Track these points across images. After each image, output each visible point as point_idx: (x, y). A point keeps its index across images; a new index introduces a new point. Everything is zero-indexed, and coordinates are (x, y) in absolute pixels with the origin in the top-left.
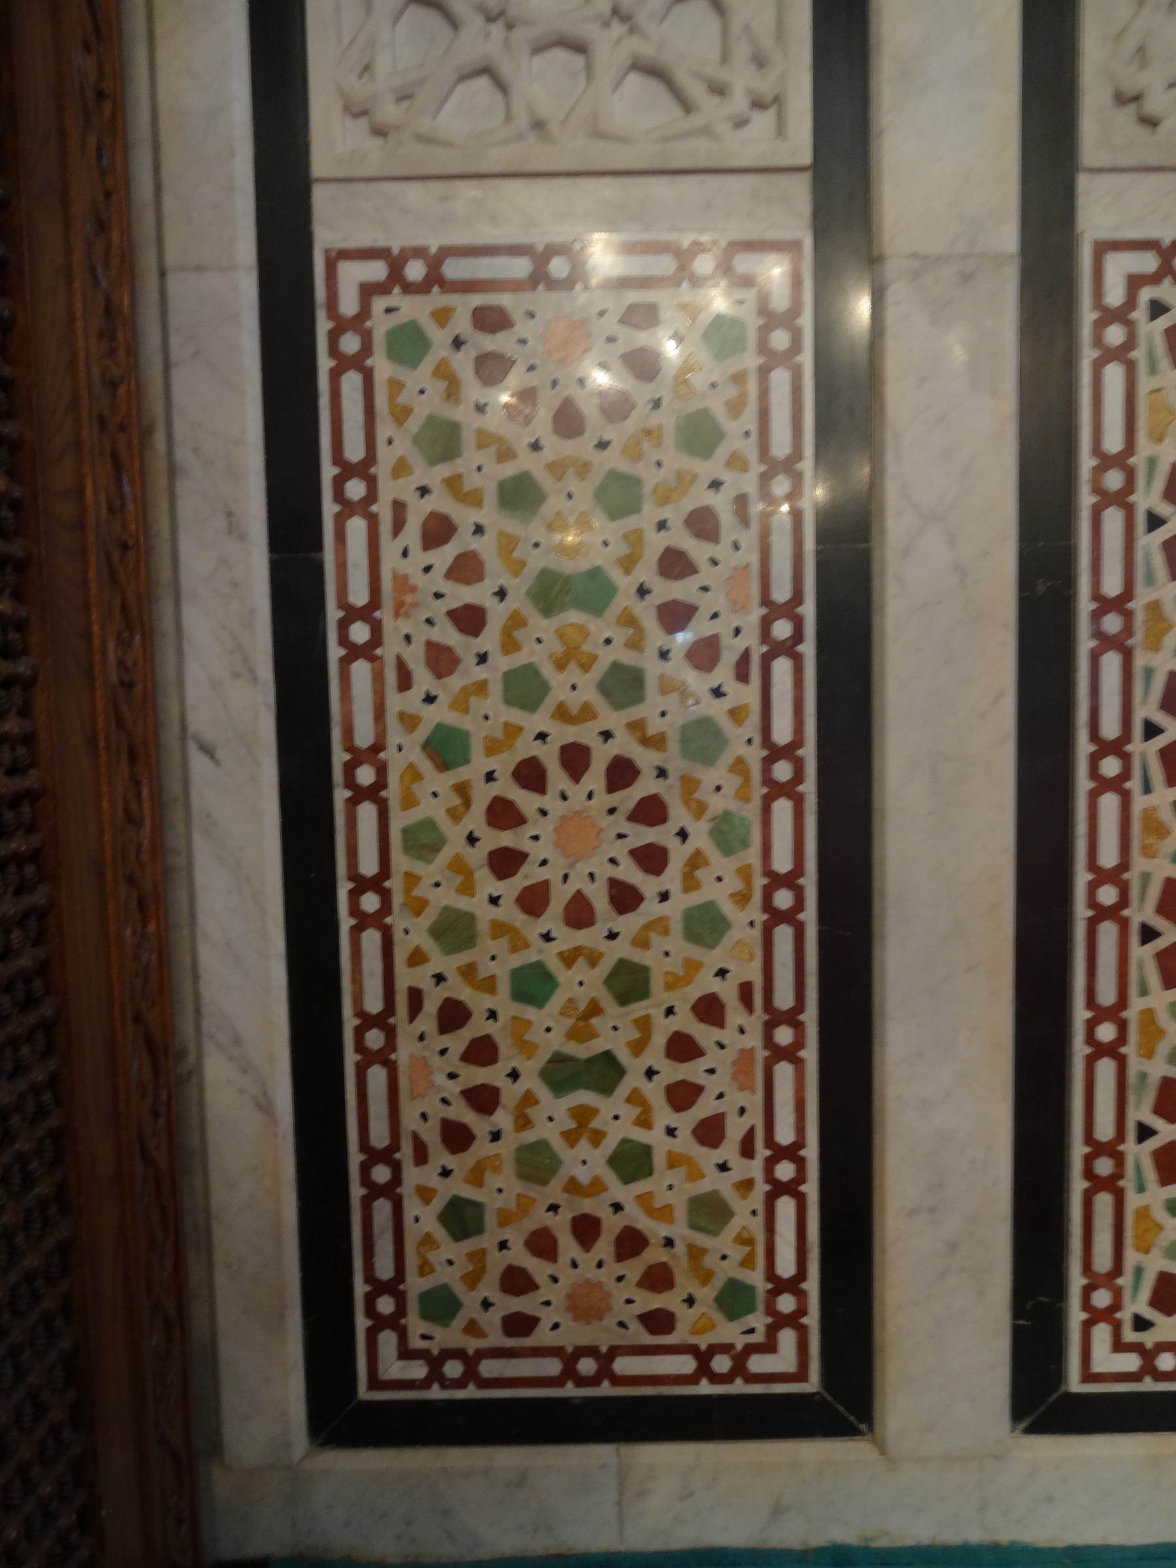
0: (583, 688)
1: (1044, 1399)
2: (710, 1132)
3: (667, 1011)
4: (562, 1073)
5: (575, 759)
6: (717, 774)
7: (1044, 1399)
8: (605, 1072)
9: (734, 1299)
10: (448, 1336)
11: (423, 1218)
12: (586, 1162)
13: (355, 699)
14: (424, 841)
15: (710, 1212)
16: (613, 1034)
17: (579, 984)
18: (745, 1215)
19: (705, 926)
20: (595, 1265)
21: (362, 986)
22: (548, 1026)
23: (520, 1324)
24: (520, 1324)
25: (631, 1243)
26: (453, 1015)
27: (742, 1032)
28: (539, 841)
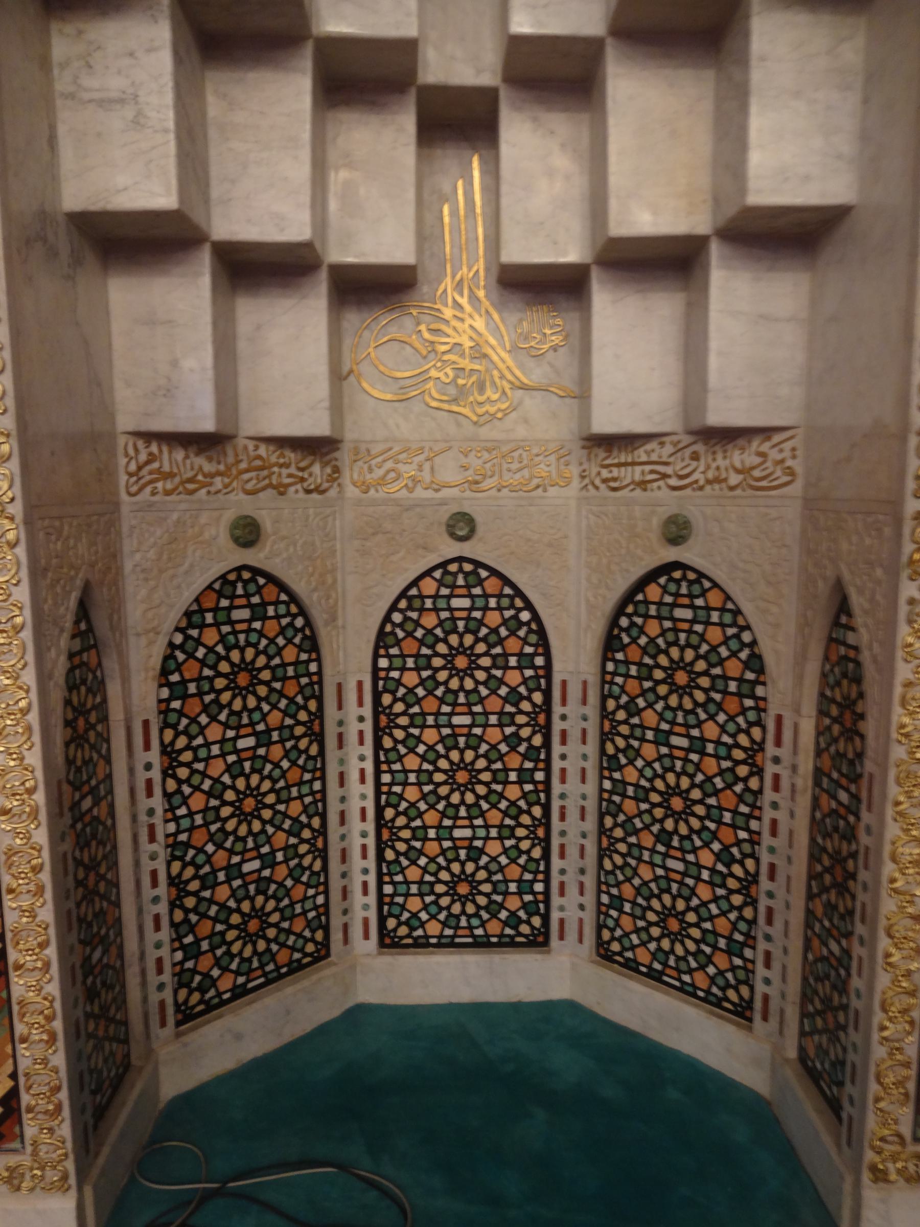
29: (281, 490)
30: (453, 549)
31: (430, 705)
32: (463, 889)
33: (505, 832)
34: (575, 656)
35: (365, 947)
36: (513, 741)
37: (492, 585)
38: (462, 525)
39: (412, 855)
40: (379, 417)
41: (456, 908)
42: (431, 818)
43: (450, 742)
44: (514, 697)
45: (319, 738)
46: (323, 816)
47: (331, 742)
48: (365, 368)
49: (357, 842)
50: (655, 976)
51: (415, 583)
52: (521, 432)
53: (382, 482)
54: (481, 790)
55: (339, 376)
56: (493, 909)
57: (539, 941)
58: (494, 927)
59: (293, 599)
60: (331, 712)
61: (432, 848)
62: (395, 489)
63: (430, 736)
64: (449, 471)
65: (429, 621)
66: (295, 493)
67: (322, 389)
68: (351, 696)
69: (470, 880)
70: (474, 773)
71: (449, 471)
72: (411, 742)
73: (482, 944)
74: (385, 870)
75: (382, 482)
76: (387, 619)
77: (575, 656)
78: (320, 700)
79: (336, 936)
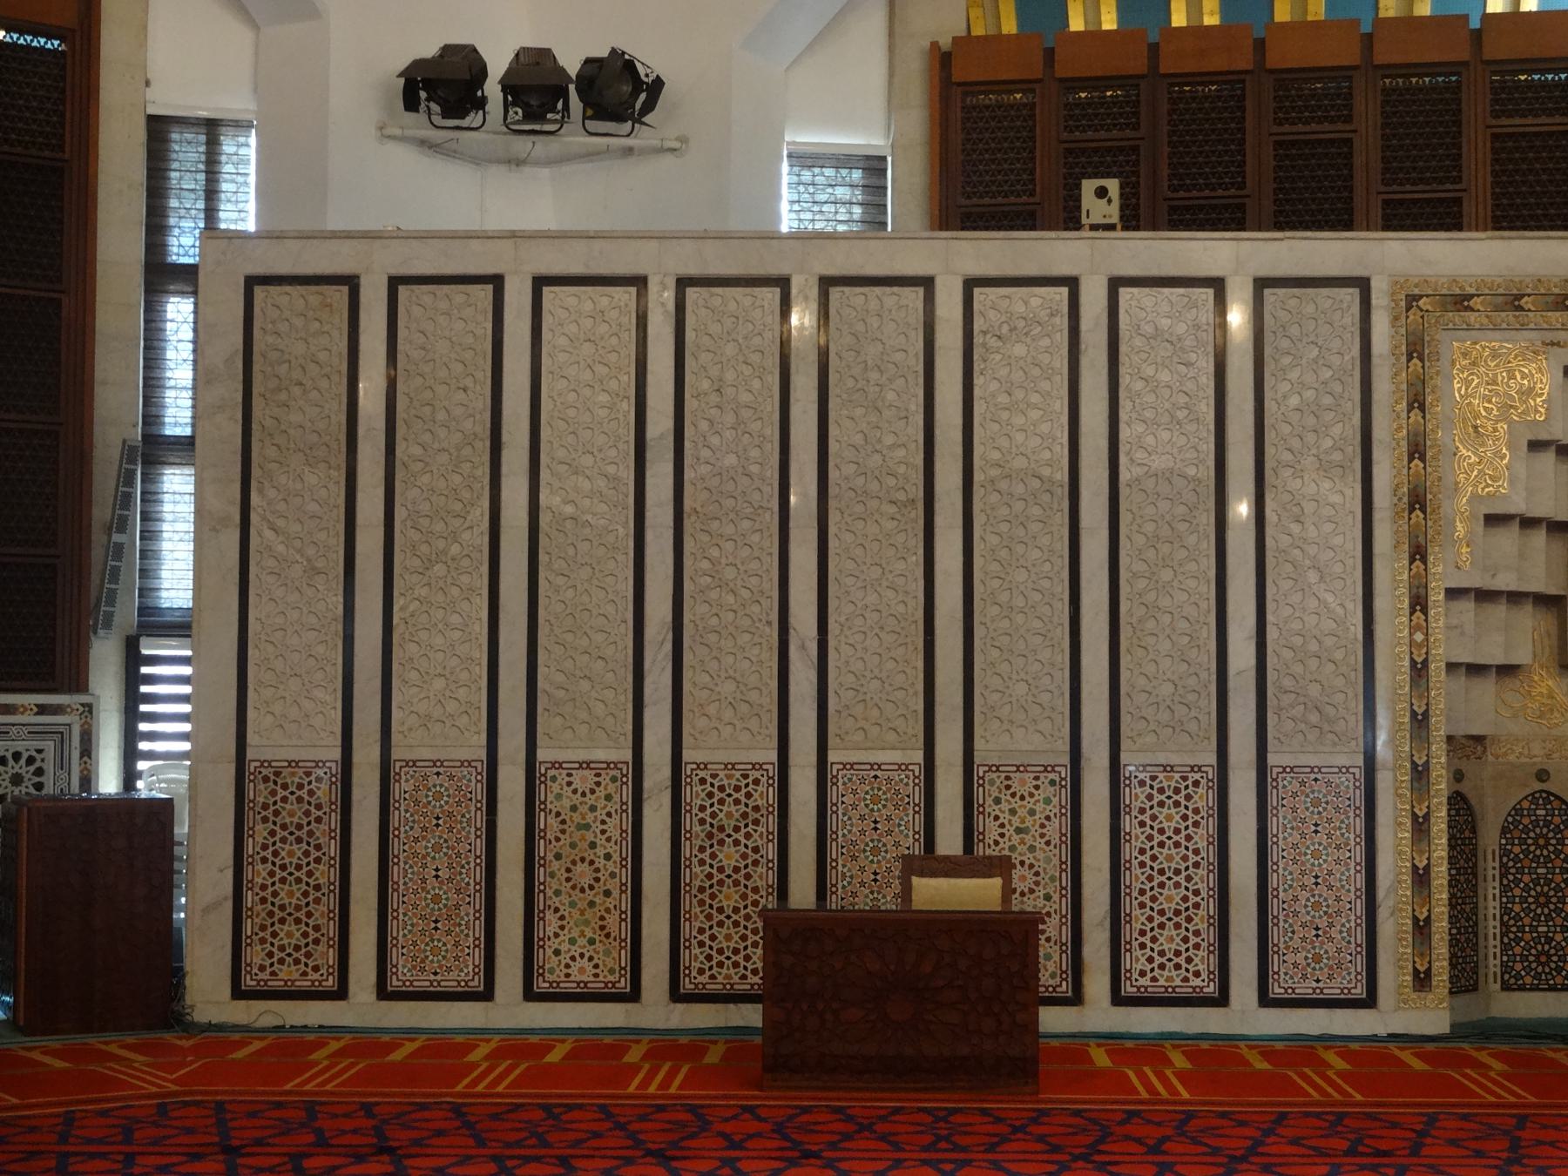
29: (1468, 757)
30: (1538, 786)
31: (1526, 863)
32: (1543, 959)
37: (1556, 804)
38: (1542, 775)
39: (1518, 940)
41: (1540, 969)
42: (1527, 921)
43: (1536, 882)
47: (1480, 878)
49: (1492, 931)
53: (1505, 754)
54: (1552, 907)
58: (1559, 980)
60: (1481, 863)
62: (1512, 758)
63: (1526, 878)
64: (1537, 749)
65: (1526, 821)
68: (1490, 857)
70: (1548, 898)
71: (1537, 749)
72: (1517, 882)
73: (1552, 989)
74: (1505, 948)
75: (1505, 754)
79: (1482, 979)
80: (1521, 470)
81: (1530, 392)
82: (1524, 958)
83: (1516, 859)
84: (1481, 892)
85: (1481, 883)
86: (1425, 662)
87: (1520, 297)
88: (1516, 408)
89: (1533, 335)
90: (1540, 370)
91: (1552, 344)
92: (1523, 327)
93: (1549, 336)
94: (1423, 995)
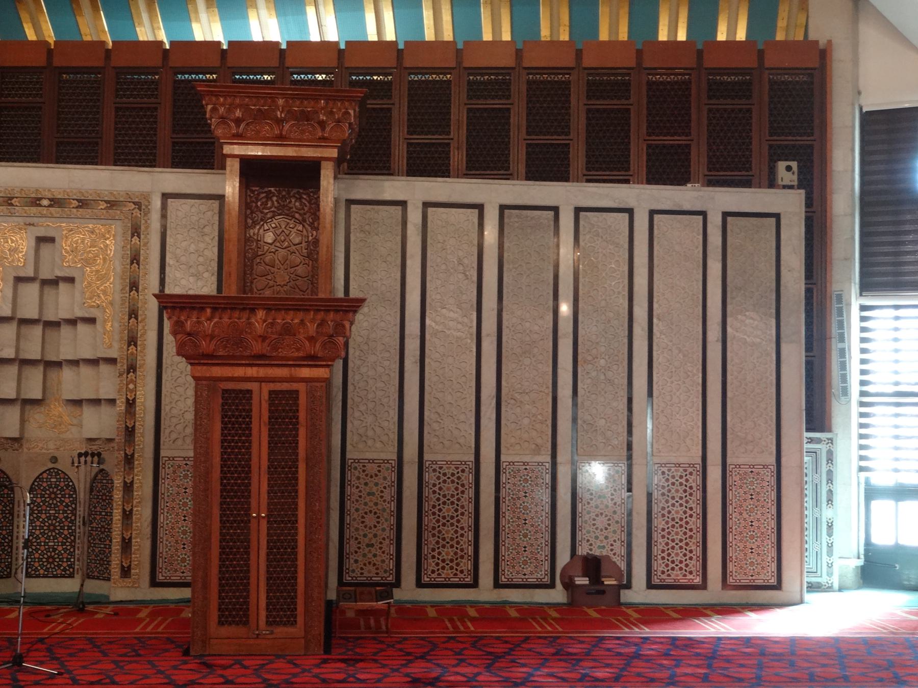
0: (371, 504)
1: (420, 584)
2: (383, 552)
3: (379, 539)
4: (368, 545)
5: (371, 512)
6: (385, 514)
7: (420, 584)
8: (372, 545)
9: (385, 571)
10: (354, 575)
11: (352, 561)
12: (370, 555)
13: (348, 504)
14: (354, 520)
15: (383, 561)
16: (373, 541)
17: (370, 536)
18: (387, 561)
19: (384, 530)
20: (371, 567)
21: (347, 536)
22: (366, 540)
23: (362, 574)
24: (362, 574)
25: (374, 565)
26: (356, 539)
27: (387, 541)
28: (367, 520)
30: (52, 466)
31: (44, 507)
33: (63, 544)
34: (82, 495)
35: (22, 576)
36: (66, 518)
37: (62, 475)
38: (54, 459)
39: (37, 550)
40: (34, 431)
44: (67, 506)
45: (12, 515)
46: (12, 536)
47: (15, 515)
48: (31, 420)
50: (98, 578)
51: (41, 474)
52: (71, 436)
55: (23, 421)
56: (59, 566)
57: (71, 576)
59: (8, 477)
61: (42, 548)
62: (37, 450)
63: (43, 516)
64: (51, 446)
65: (45, 485)
66: (10, 450)
67: (18, 426)
69: (53, 557)
73: (55, 577)
76: (33, 484)
77: (82, 495)
78: (13, 505)
80: (9, 293)
81: (14, 250)
82: (40, 560)
83: (38, 506)
84: (15, 523)
85: (16, 519)
86: (134, 400)
87: (11, 198)
88: (7, 259)
89: (20, 219)
90: (21, 238)
91: (30, 224)
92: (12, 215)
93: (29, 220)
94: (126, 580)
